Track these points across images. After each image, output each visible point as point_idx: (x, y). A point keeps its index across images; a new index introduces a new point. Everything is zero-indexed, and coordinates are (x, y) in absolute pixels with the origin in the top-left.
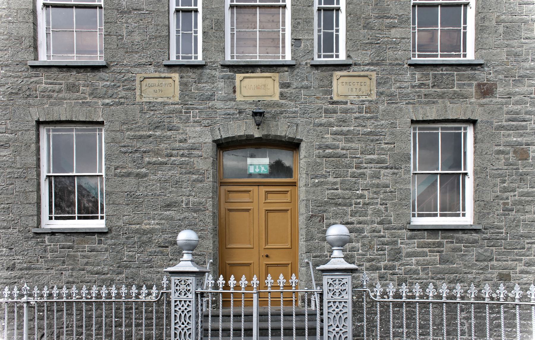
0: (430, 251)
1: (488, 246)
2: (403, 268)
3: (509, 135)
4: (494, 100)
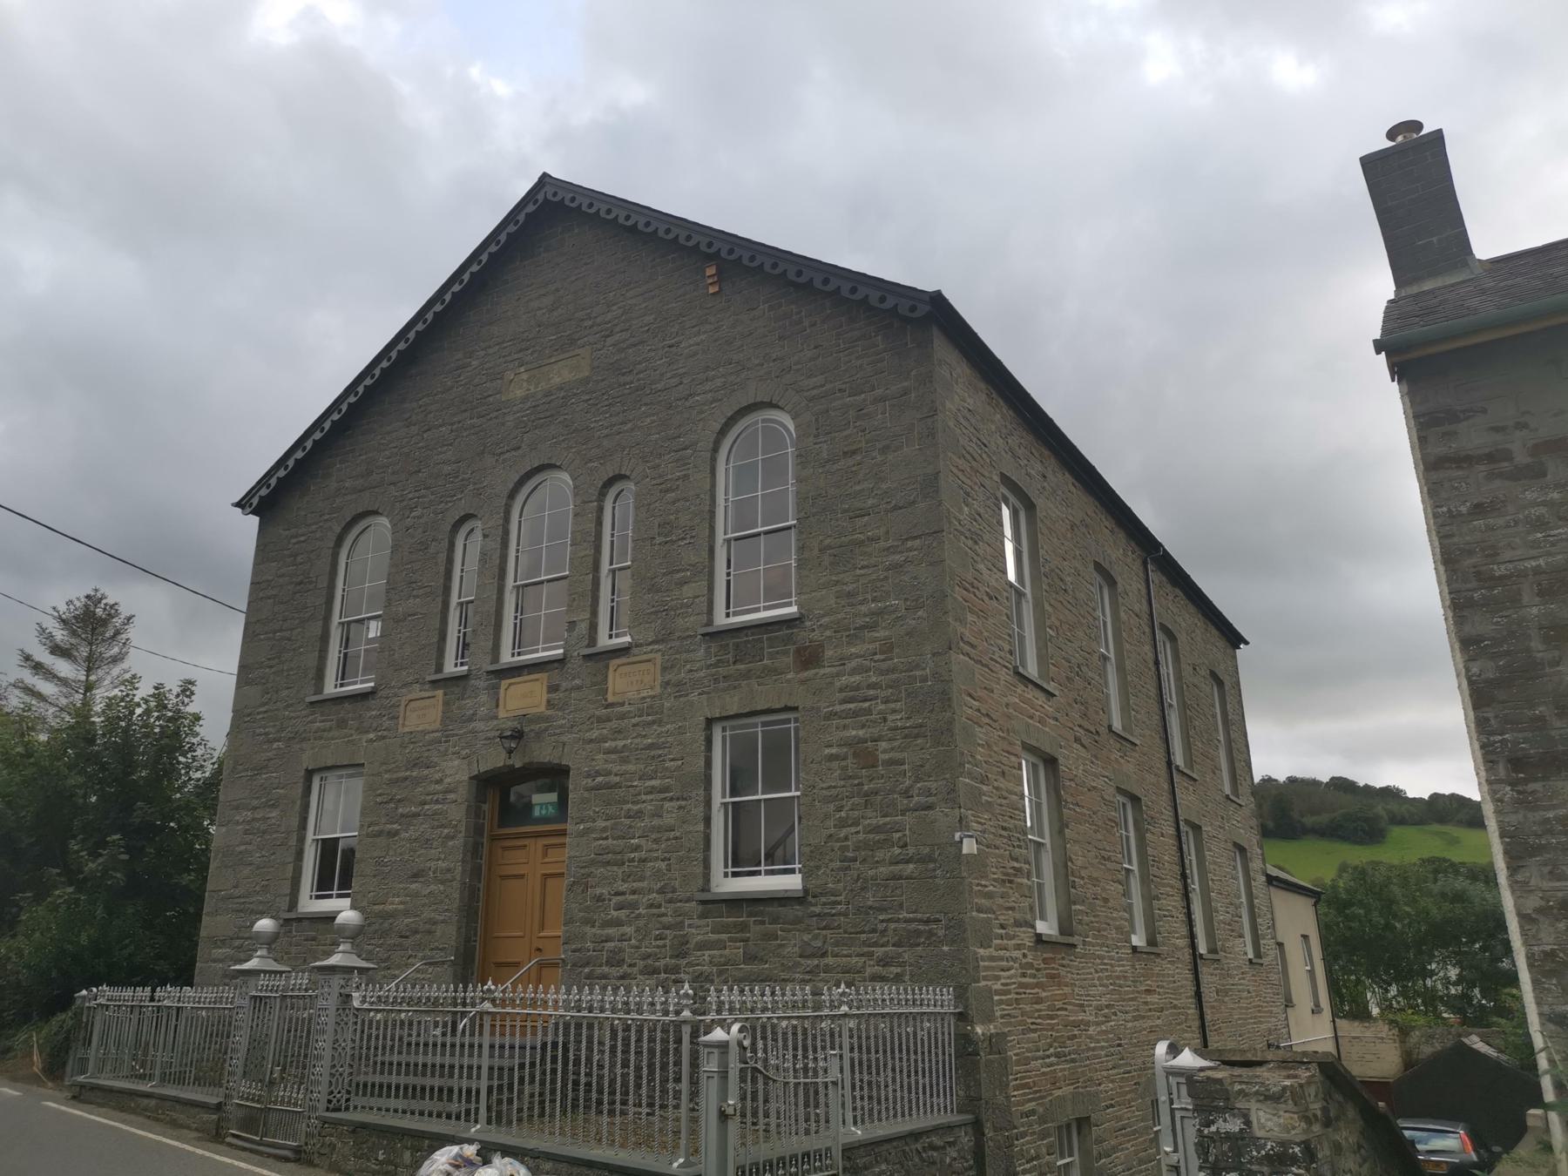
0: (731, 940)
1: (818, 929)
2: (691, 969)
3: (845, 727)
4: (822, 671)
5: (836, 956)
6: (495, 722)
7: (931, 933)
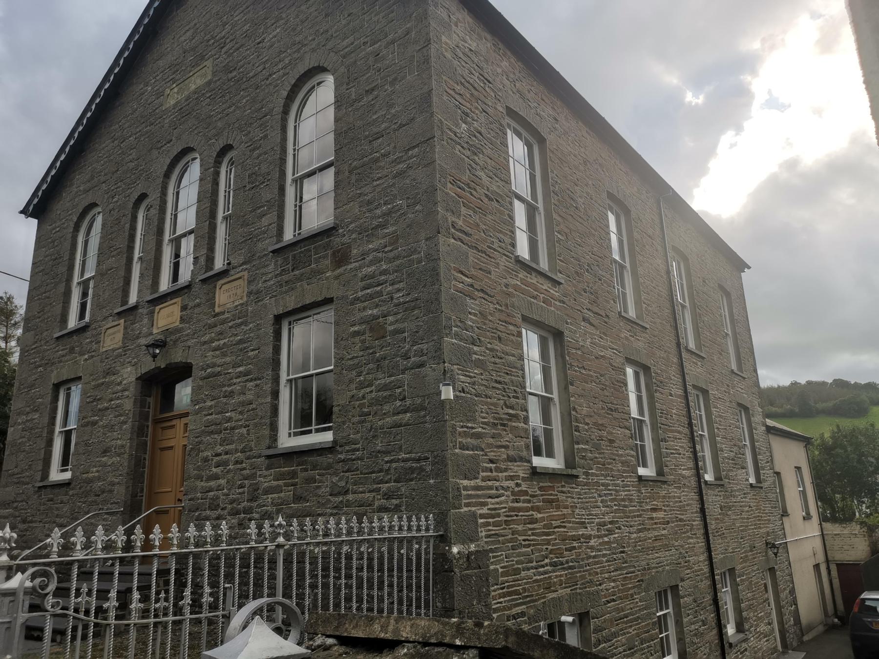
0: (286, 485)
1: (343, 472)
3: (364, 309)
4: (349, 267)
5: (355, 493)
6: (151, 337)
7: (421, 469)
